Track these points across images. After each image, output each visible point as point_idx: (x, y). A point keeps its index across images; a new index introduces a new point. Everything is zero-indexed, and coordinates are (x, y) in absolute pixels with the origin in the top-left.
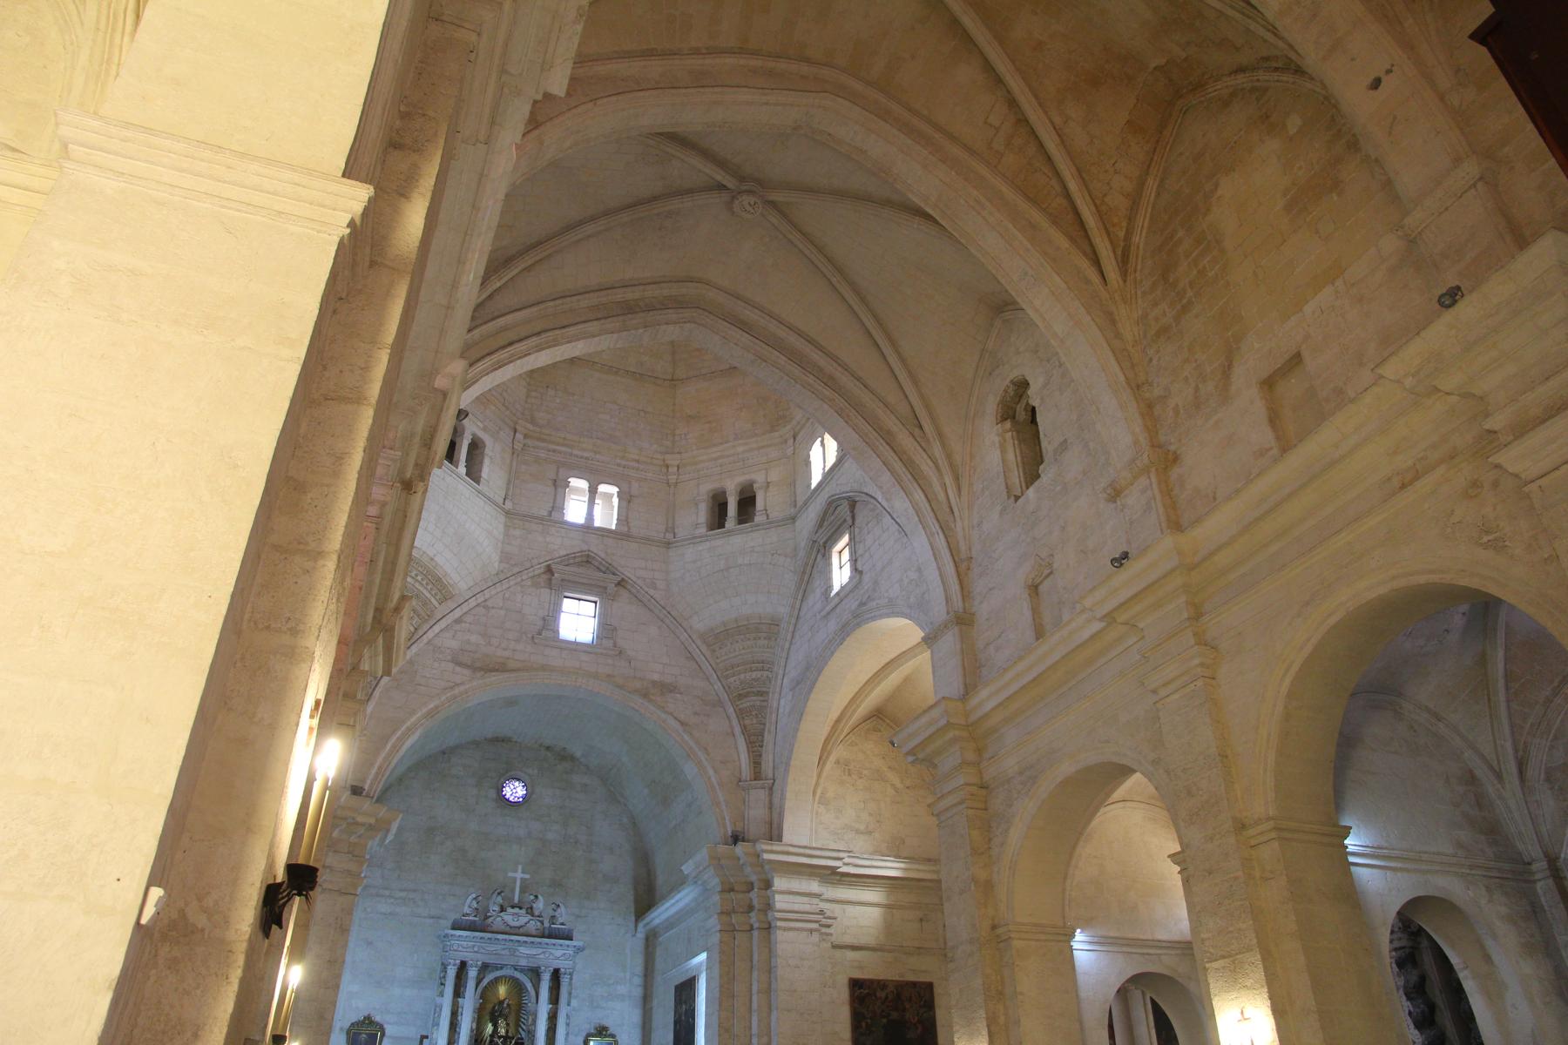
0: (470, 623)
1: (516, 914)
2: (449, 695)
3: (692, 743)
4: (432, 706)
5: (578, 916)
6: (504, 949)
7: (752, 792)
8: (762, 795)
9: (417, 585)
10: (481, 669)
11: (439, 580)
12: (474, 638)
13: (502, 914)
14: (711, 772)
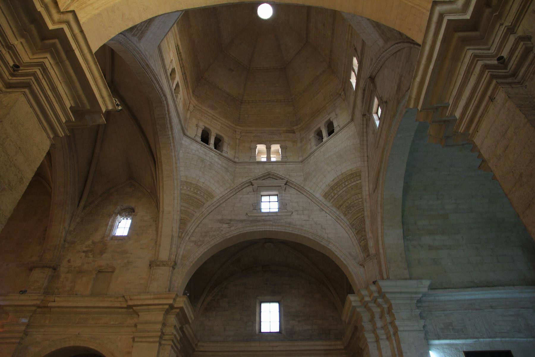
11: (352, 174)
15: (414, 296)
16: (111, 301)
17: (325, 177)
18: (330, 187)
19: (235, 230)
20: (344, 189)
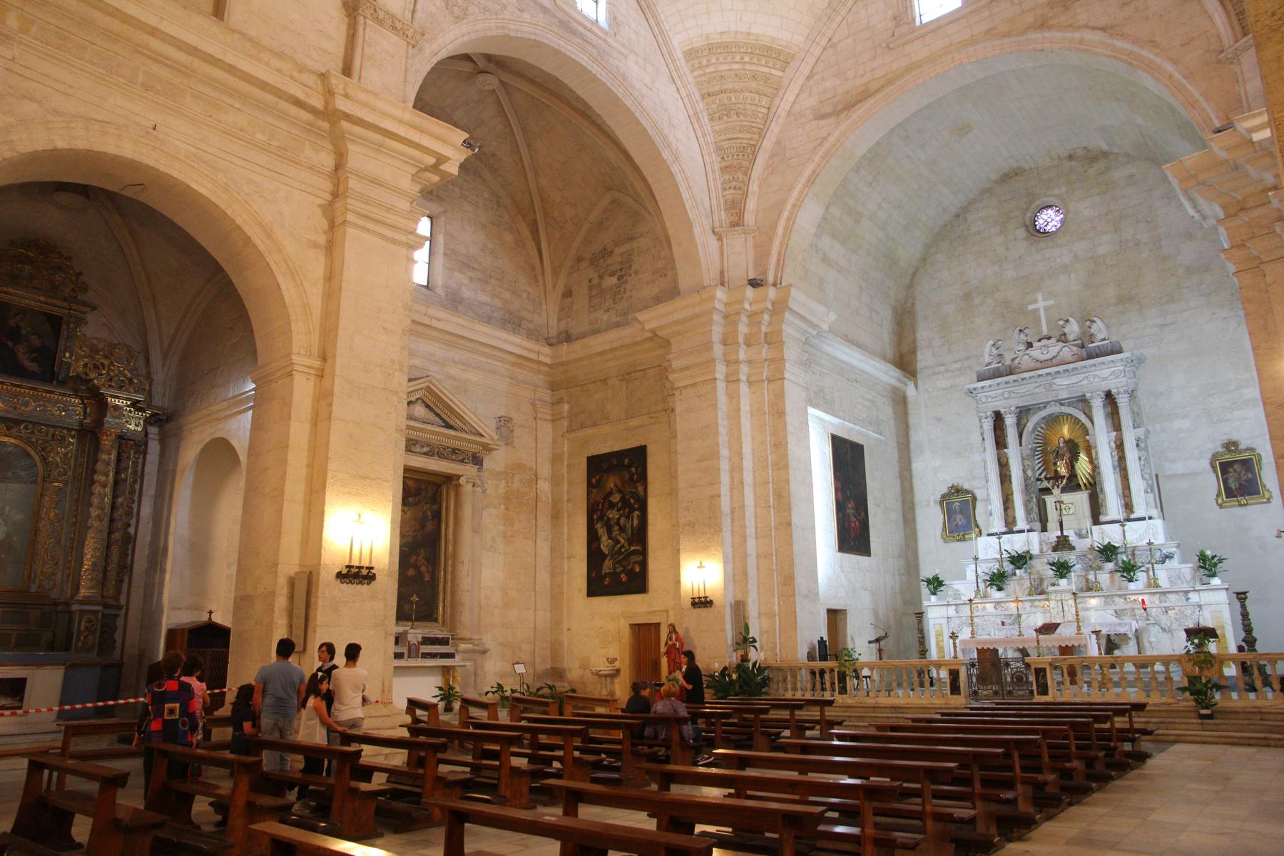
0: (822, 72)
1: (1044, 346)
2: (820, 153)
3: (1128, 46)
4: (807, 173)
5: (1163, 326)
6: (1037, 387)
9: (748, 67)
10: (844, 109)
11: (769, 49)
12: (828, 84)
13: (1028, 352)
14: (1169, 68)
15: (810, 330)
16: (279, 70)
17: (708, 13)
18: (706, 43)
19: (530, 23)
20: (735, 66)
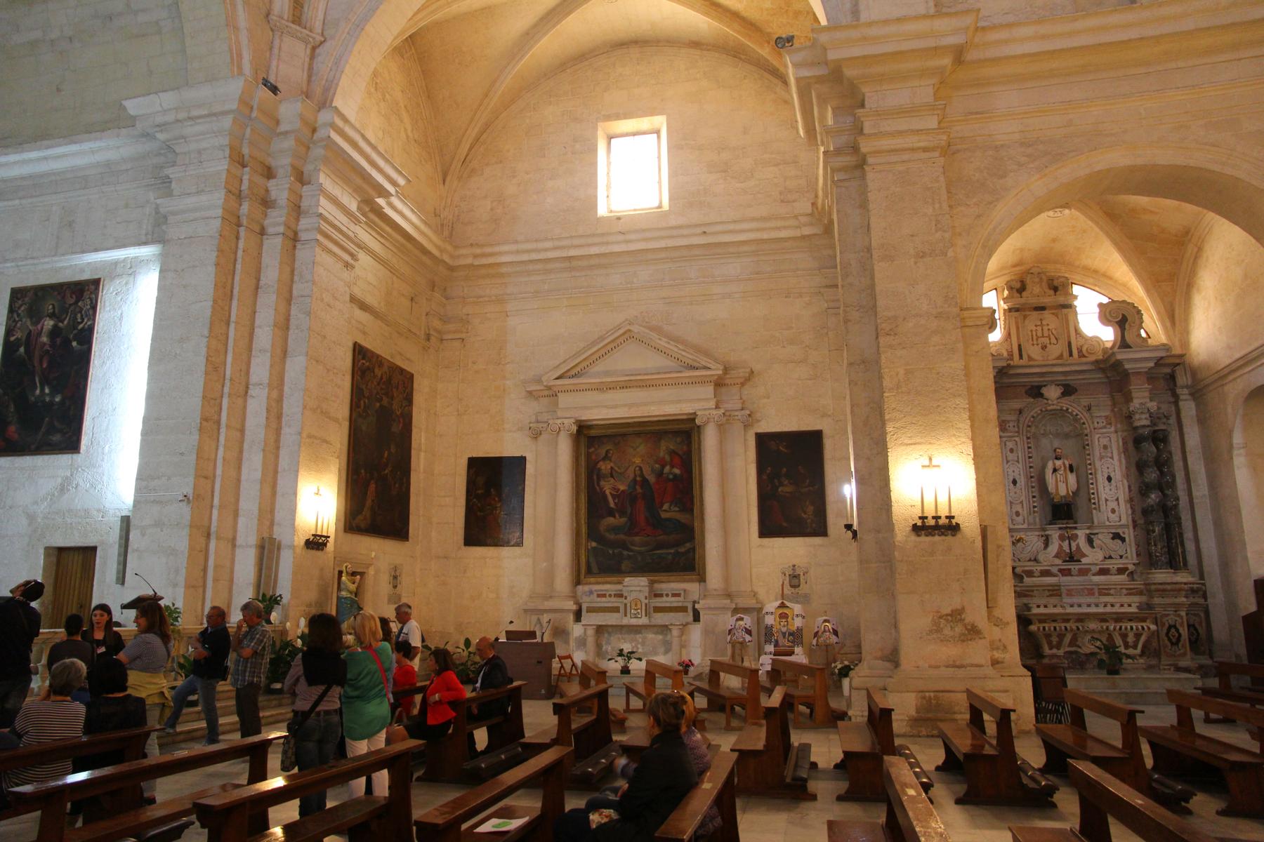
7: (287, 40)
8: (302, 51)
